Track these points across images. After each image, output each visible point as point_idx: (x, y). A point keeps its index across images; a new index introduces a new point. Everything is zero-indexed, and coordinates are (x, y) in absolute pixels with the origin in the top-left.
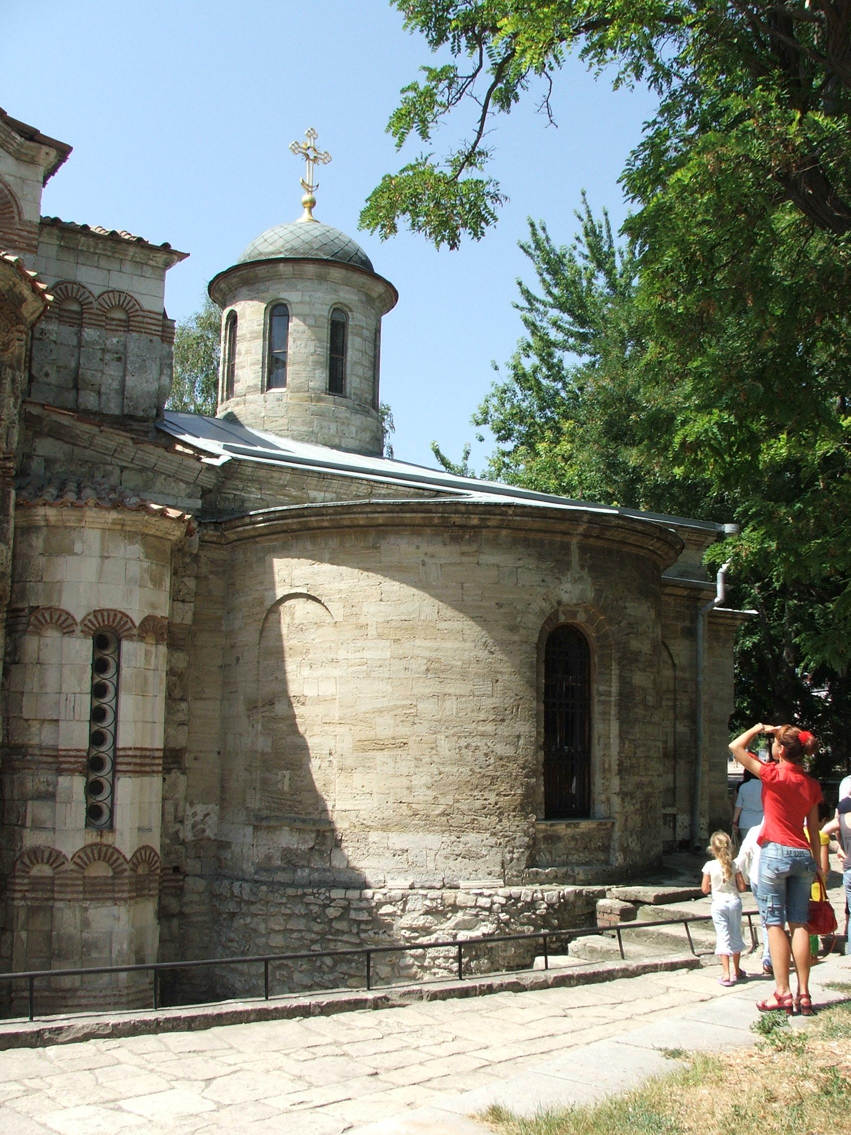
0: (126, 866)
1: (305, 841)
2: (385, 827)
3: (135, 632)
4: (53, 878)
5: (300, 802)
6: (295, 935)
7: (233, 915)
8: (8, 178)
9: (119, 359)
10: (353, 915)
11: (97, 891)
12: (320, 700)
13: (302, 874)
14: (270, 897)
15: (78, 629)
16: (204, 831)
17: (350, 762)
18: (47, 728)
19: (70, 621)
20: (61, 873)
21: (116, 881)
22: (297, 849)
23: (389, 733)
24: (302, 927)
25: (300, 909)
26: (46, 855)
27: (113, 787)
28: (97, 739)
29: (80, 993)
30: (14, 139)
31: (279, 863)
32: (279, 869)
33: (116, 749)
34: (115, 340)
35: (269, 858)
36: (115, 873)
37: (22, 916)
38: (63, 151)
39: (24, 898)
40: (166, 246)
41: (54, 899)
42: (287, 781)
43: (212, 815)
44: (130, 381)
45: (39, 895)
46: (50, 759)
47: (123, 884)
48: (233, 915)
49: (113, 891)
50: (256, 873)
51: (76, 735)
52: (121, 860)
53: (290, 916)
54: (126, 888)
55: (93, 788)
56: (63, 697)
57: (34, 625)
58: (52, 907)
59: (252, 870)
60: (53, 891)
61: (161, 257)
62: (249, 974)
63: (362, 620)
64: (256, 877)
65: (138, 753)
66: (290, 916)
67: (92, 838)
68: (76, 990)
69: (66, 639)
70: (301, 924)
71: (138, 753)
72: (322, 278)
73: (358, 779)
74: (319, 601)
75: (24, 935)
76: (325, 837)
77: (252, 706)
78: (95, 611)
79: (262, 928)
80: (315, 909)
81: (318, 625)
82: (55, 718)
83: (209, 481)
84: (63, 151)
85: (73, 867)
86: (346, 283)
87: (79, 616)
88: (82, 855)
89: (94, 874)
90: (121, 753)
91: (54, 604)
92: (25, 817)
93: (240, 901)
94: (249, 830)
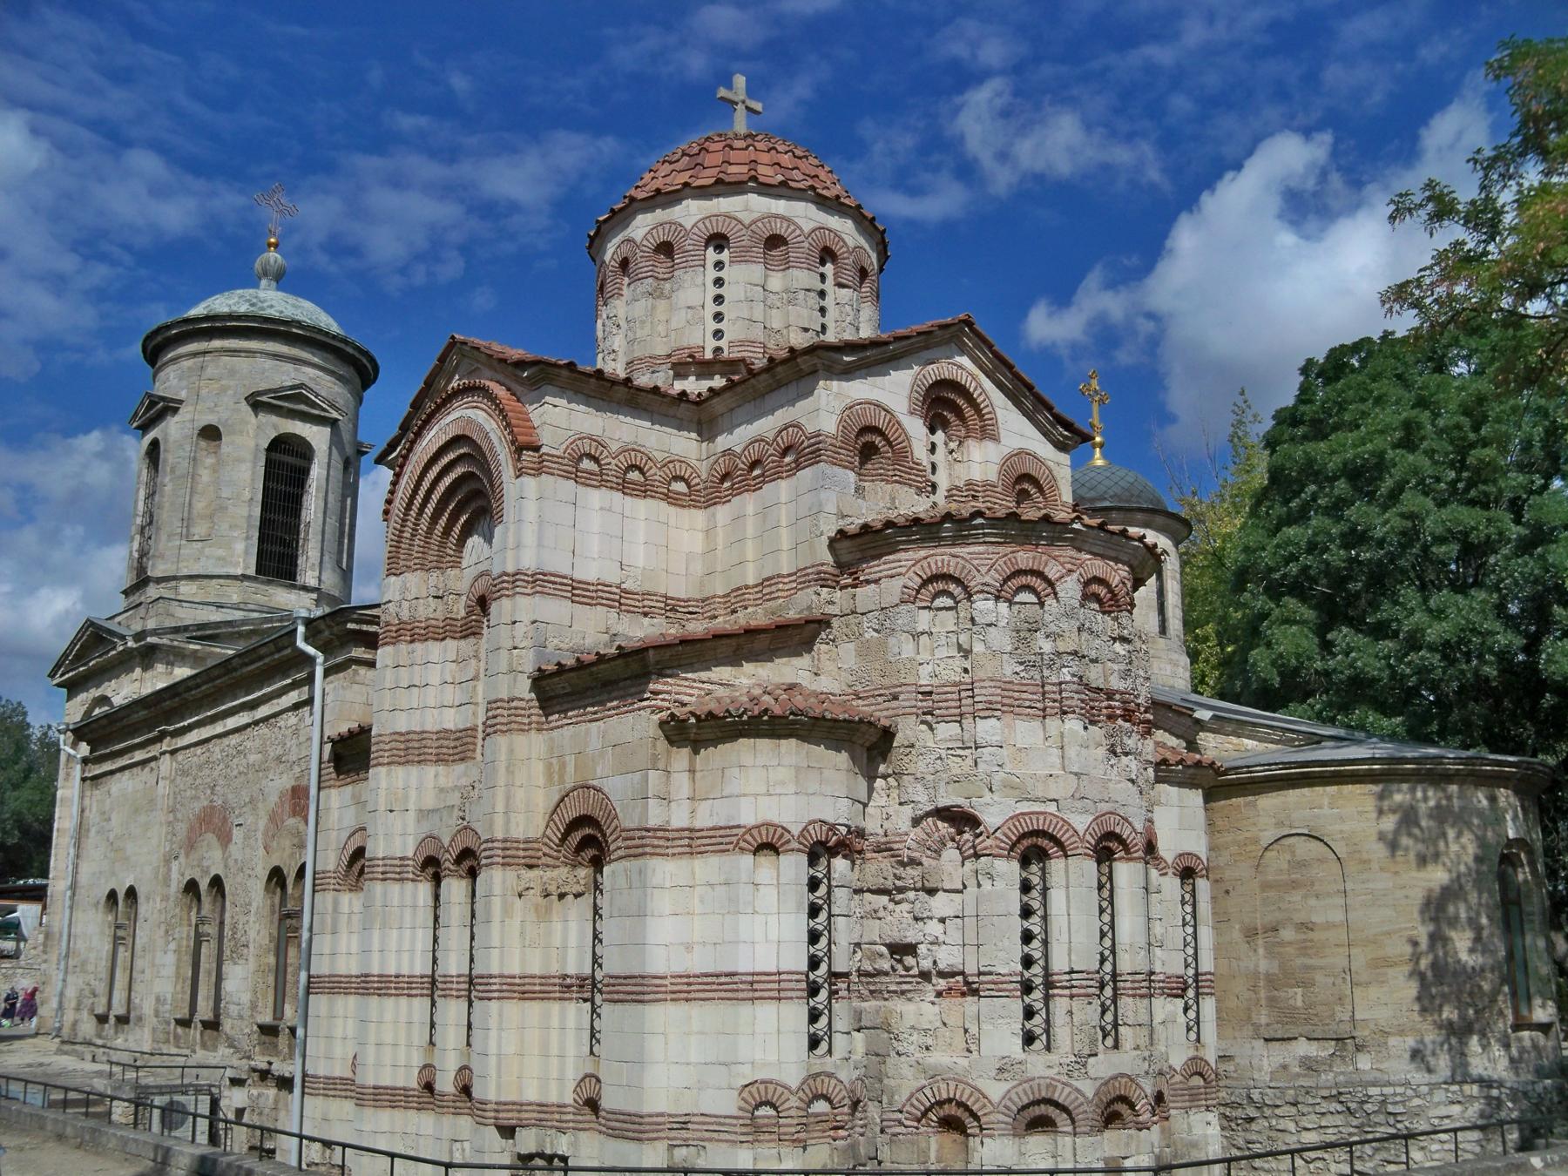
1: (1325, 1049)
6: (1330, 1131)
7: (1251, 1120)
8: (1050, 464)
10: (1391, 1108)
12: (1330, 926)
13: (1327, 1078)
17: (1364, 976)
25: (1335, 1106)
32: (1298, 1075)
35: (1285, 1067)
42: (1299, 998)
48: (1251, 1120)
63: (1365, 856)
67: (1192, 1053)
70: (1338, 1120)
73: (1374, 992)
79: (1292, 1127)
80: (1353, 1106)
81: (1321, 861)
87: (1170, 862)
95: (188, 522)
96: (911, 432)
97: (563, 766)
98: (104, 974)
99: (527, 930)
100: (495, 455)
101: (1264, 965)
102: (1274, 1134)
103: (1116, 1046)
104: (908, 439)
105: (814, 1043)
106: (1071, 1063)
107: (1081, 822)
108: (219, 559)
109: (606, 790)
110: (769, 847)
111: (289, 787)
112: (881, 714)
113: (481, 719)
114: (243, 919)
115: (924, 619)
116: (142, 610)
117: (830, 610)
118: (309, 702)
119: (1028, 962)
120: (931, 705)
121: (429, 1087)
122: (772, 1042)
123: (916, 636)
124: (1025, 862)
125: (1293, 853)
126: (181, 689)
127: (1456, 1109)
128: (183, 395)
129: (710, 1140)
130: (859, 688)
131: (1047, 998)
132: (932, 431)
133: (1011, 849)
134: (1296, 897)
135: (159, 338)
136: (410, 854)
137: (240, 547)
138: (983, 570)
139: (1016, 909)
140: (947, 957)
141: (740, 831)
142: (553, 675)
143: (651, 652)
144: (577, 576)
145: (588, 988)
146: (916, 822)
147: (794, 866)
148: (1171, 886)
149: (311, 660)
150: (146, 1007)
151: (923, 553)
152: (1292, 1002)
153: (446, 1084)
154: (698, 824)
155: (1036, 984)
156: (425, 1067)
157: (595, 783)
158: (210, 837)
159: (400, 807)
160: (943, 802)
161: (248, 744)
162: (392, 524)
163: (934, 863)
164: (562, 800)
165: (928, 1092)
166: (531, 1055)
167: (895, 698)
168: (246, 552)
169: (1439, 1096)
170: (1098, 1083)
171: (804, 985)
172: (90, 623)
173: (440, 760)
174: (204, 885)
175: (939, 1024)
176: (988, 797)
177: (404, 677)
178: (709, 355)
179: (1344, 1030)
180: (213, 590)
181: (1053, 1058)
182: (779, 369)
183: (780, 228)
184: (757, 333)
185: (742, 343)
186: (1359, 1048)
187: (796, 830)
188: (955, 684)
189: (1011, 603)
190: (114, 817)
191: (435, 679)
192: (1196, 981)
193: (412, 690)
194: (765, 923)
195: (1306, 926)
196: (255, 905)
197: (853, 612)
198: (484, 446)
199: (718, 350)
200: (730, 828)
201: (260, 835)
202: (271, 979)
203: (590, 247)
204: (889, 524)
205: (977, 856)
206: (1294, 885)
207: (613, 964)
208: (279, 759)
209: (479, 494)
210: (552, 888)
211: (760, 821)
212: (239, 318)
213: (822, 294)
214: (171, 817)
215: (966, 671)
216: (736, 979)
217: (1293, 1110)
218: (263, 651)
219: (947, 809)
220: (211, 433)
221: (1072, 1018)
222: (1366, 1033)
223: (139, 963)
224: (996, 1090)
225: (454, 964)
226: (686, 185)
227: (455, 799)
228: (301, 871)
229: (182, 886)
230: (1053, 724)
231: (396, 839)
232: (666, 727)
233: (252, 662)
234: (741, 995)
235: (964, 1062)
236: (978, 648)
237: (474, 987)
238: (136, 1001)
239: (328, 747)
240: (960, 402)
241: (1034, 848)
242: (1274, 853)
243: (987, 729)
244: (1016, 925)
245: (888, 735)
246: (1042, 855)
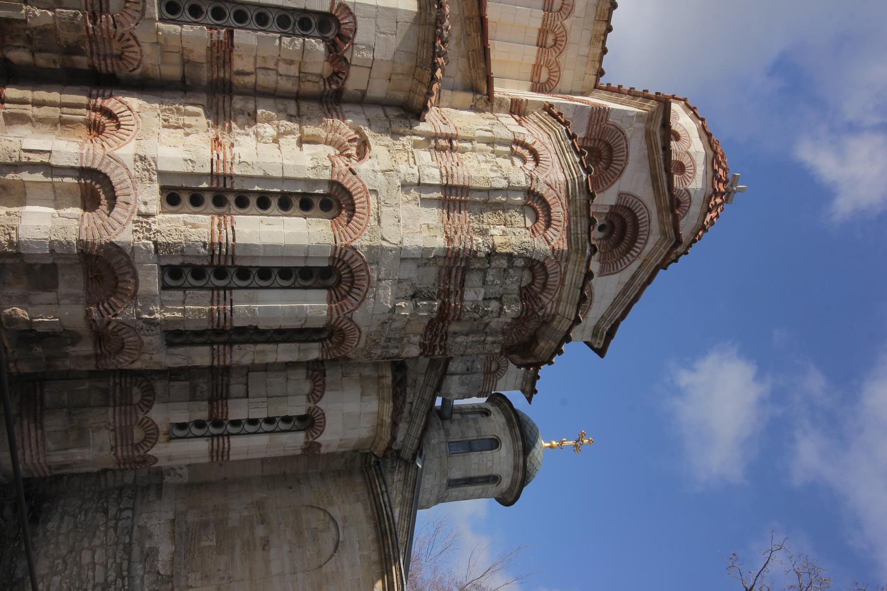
0: (142, 452)
3: (311, 439)
4: (131, 404)
5: (193, 558)
6: (91, 573)
7: (106, 511)
9: (468, 370)
11: (122, 434)
14: (121, 547)
15: (312, 405)
16: (169, 475)
18: (243, 387)
19: (316, 398)
20: (135, 409)
21: (130, 447)
22: (158, 561)
24: (97, 580)
26: (149, 398)
27: (202, 436)
28: (236, 423)
29: (39, 432)
30: (607, 325)
31: (147, 546)
33: (229, 435)
34: (479, 366)
35: (150, 536)
36: (136, 445)
37: (102, 385)
38: (601, 352)
39: (115, 384)
40: (536, 392)
41: (114, 406)
43: (181, 480)
44: (456, 378)
45: (118, 394)
46: (220, 391)
47: (127, 452)
48: (106, 511)
49: (122, 446)
50: (138, 526)
51: (238, 410)
52: (146, 449)
54: (125, 454)
55: (200, 424)
56: (265, 399)
57: (312, 375)
58: (108, 406)
60: (121, 405)
61: (528, 389)
62: (59, 534)
64: (136, 528)
65: (226, 450)
66: (106, 567)
67: (163, 428)
68: (42, 428)
69: (304, 398)
70: (100, 579)
71: (226, 450)
72: (516, 467)
75: (86, 386)
76: (168, 582)
77: (260, 505)
78: (324, 414)
79: (96, 542)
82: (250, 394)
83: (407, 454)
84: (601, 352)
85: (140, 418)
86: (513, 482)
87: (318, 405)
88: (150, 423)
89: (135, 431)
90: (226, 440)
91: (327, 388)
92: (177, 380)
93: (117, 519)
94: (171, 516)
96: (607, 192)
104: (603, 191)
133: (339, 185)
138: (548, 180)
151: (550, 147)
152: (204, 538)
170: (128, 252)
183: (689, 170)
192: (222, 435)
195: (266, 544)
240: (623, 246)
242: (322, 517)
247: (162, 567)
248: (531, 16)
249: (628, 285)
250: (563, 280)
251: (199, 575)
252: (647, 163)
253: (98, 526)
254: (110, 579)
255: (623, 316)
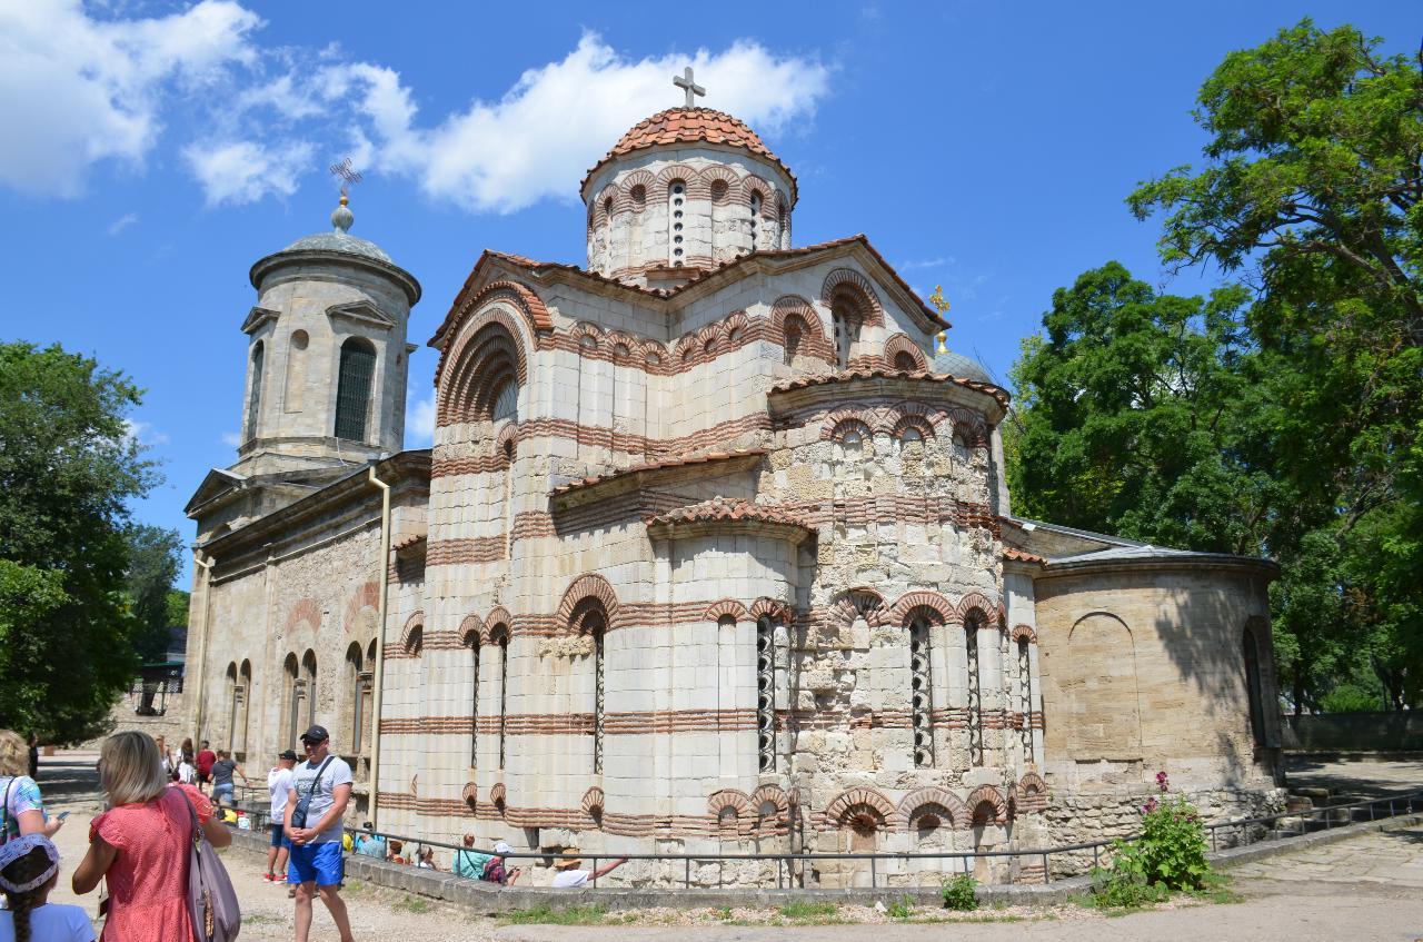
2: (1177, 756)
7: (1066, 819)
12: (1123, 679)
23: (1172, 697)
25: (1128, 808)
48: (1066, 819)
53: (1120, 815)
59: (1079, 789)
66: (1120, 815)
70: (1130, 819)
73: (1156, 726)
74: (1116, 617)
79: (1097, 823)
80: (1142, 808)
81: (1119, 631)
84: (946, 326)
95: (285, 400)
97: (573, 562)
98: (228, 723)
99: (547, 678)
100: (519, 335)
101: (1076, 707)
102: (1084, 829)
103: (980, 763)
105: (763, 761)
106: (949, 774)
107: (955, 600)
108: (308, 426)
109: (606, 577)
110: (727, 619)
111: (363, 583)
112: (810, 519)
113: (510, 527)
114: (329, 681)
115: (837, 452)
116: (251, 463)
117: (768, 445)
118: (379, 523)
119: (917, 701)
120: (845, 517)
121: (471, 801)
122: (732, 763)
123: (833, 465)
124: (914, 629)
125: (1095, 626)
126: (282, 516)
127: (1215, 811)
128: (280, 308)
129: (685, 835)
130: (790, 503)
131: (931, 730)
132: (836, 319)
133: (907, 617)
134: (1098, 658)
135: (262, 268)
136: (457, 629)
137: (323, 416)
139: (909, 663)
140: (857, 698)
141: (707, 606)
142: (565, 493)
143: (641, 475)
144: (581, 424)
145: (591, 724)
146: (835, 600)
147: (747, 631)
148: (1014, 647)
149: (380, 491)
150: (256, 744)
153: (484, 797)
154: (675, 601)
155: (923, 718)
156: (469, 784)
157: (598, 572)
158: (305, 622)
159: (451, 595)
160: (854, 585)
161: (333, 553)
162: (441, 389)
163: (848, 630)
164: (572, 586)
165: (845, 798)
166: (550, 775)
167: (817, 509)
168: (328, 420)
169: (1205, 800)
171: (755, 719)
172: (214, 475)
173: (480, 560)
174: (300, 658)
175: (852, 748)
176: (887, 582)
177: (454, 499)
178: (672, 265)
179: (1135, 755)
180: (303, 449)
181: (937, 772)
182: (729, 272)
184: (707, 251)
185: (696, 257)
186: (1145, 767)
187: (749, 607)
188: (861, 499)
189: (902, 443)
190: (233, 609)
191: (475, 502)
193: (458, 508)
194: (726, 670)
195: (1104, 679)
196: (338, 670)
197: (784, 448)
198: (511, 330)
199: (678, 263)
200: (700, 603)
201: (342, 620)
202: (351, 724)
203: (582, 191)
204: (812, 383)
205: (880, 624)
206: (1096, 649)
207: (611, 705)
208: (355, 563)
209: (507, 365)
210: (566, 651)
211: (723, 598)
212: (321, 251)
213: (753, 224)
214: (275, 608)
215: (869, 489)
216: (706, 715)
217: (1098, 812)
218: (344, 485)
219: (857, 590)
220: (301, 339)
221: (949, 743)
222: (1151, 756)
223: (252, 715)
224: (895, 796)
225: (489, 708)
226: (654, 143)
227: (490, 587)
228: (374, 642)
229: (284, 658)
230: (934, 528)
231: (446, 618)
232: (652, 530)
233: (337, 494)
234: (709, 727)
235: (873, 776)
236: (879, 473)
237: (504, 725)
238: (250, 741)
239: (393, 555)
240: (857, 298)
241: (921, 620)
243: (884, 533)
244: (909, 675)
245: (813, 535)
246: (928, 624)
247: (1120, 769)
248: (604, 375)
249: (891, 294)
250: (965, 407)
251: (1130, 738)
252: (800, 272)
253: (1082, 824)
254: (1133, 810)
255: (920, 303)
